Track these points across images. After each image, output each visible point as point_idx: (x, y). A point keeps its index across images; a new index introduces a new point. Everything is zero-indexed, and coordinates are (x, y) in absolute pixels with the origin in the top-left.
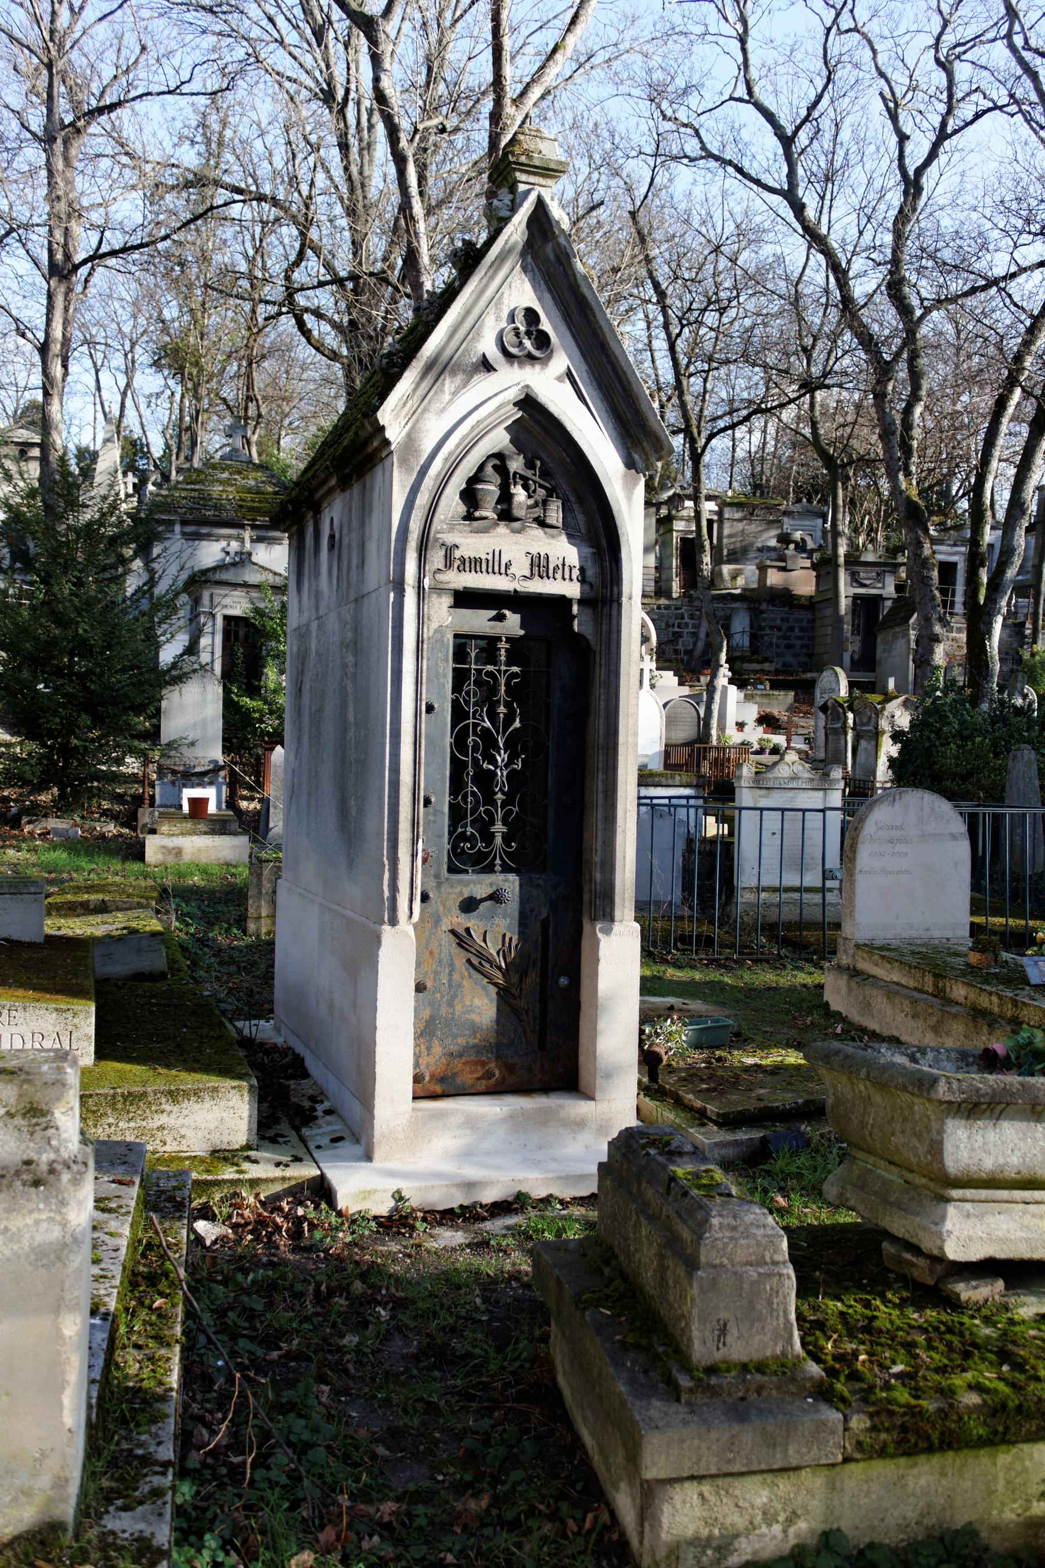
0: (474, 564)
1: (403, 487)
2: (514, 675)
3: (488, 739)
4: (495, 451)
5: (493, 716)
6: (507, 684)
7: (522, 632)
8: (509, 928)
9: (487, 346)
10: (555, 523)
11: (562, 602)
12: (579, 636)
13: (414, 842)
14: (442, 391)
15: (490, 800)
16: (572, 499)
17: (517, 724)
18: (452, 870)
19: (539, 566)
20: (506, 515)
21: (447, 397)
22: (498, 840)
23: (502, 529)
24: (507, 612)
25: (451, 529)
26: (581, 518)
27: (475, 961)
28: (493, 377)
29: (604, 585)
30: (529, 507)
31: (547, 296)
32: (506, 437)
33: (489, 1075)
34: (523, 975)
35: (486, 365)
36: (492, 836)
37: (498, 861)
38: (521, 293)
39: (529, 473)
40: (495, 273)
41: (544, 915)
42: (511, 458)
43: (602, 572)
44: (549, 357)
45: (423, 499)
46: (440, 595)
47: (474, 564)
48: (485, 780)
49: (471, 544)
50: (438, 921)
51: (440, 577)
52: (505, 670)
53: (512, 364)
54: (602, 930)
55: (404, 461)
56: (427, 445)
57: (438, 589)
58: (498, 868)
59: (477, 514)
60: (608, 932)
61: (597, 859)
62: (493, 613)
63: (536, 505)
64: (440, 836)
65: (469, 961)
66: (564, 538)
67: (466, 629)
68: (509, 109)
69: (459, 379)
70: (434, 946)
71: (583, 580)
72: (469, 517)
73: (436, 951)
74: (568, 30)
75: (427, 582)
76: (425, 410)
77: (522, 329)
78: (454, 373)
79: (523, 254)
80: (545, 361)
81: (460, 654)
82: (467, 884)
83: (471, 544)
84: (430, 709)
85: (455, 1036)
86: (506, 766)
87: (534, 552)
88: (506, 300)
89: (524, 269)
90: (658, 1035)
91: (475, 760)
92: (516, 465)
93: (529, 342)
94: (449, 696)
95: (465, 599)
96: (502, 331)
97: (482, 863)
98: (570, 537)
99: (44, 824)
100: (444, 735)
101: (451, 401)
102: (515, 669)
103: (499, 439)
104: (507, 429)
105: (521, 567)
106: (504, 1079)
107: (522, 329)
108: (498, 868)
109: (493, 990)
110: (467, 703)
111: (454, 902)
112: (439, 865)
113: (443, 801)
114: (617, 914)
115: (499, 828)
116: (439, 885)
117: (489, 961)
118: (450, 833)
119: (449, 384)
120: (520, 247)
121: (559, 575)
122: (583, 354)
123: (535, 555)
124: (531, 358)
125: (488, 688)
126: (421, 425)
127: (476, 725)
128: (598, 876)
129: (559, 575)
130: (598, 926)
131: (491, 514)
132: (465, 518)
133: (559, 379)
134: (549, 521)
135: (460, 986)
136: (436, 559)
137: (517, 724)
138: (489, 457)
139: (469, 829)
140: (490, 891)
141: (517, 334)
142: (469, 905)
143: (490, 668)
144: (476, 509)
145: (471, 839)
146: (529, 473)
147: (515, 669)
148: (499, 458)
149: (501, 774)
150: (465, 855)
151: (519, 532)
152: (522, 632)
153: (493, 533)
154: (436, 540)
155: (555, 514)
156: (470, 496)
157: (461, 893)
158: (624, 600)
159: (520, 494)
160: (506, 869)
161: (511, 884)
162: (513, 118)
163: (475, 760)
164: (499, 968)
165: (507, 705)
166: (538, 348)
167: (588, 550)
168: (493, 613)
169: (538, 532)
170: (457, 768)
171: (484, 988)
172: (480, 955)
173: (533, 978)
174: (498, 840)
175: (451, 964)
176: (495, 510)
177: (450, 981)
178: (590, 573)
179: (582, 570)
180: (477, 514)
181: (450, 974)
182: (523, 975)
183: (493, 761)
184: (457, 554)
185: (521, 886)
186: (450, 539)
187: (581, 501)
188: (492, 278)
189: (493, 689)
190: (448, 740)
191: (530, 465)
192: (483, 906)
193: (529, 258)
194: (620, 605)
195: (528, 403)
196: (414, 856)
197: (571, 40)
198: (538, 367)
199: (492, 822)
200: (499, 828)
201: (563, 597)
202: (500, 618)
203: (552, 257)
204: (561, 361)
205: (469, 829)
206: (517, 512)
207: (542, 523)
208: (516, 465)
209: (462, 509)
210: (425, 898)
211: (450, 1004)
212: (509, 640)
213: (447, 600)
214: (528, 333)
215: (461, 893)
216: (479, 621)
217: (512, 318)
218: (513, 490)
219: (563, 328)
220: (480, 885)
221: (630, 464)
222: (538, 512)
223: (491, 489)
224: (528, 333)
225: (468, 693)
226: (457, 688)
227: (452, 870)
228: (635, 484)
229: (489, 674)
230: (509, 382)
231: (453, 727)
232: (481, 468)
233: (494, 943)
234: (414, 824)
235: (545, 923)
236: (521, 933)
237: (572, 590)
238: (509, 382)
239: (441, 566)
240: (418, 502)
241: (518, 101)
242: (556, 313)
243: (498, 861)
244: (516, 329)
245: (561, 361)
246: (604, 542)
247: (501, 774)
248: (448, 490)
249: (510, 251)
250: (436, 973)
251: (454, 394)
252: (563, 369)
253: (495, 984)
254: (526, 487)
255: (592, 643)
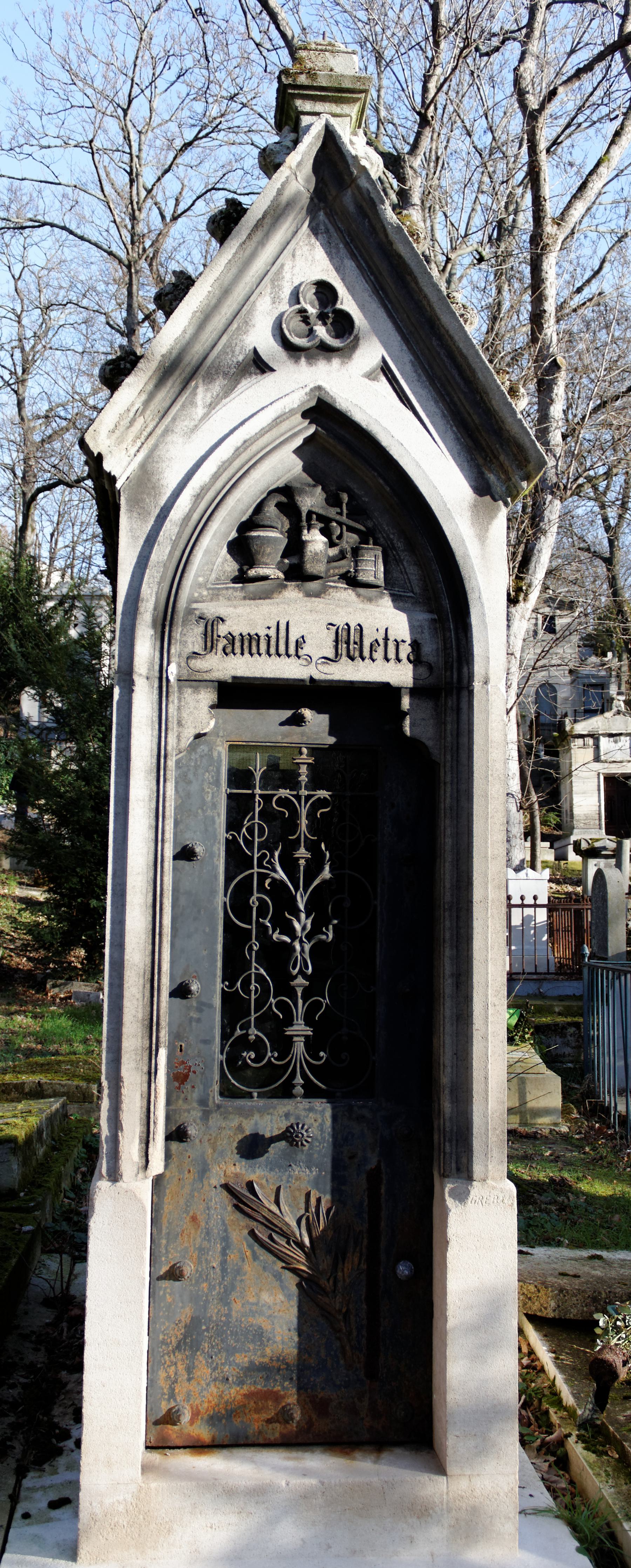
0: (249, 643)
1: (135, 538)
2: (322, 803)
3: (282, 899)
4: (280, 483)
5: (290, 865)
6: (311, 815)
7: (332, 740)
8: (316, 1183)
9: (260, 337)
10: (371, 579)
11: (386, 693)
12: (413, 741)
13: (152, 1053)
14: (193, 403)
15: (284, 987)
16: (399, 545)
17: (326, 873)
18: (228, 1092)
19: (348, 642)
20: (296, 572)
21: (200, 411)
22: (299, 1047)
23: (292, 593)
24: (307, 713)
25: (215, 595)
26: (413, 572)
27: (263, 1235)
28: (268, 379)
29: (448, 666)
30: (331, 560)
31: (350, 264)
32: (296, 466)
33: (284, 1416)
34: (339, 1256)
35: (259, 365)
36: (289, 1042)
37: (299, 1080)
38: (310, 262)
39: (332, 512)
40: (267, 236)
41: (373, 1163)
42: (301, 492)
43: (446, 648)
44: (353, 347)
45: (161, 553)
46: (196, 690)
47: (249, 643)
48: (277, 958)
49: (243, 615)
50: (204, 1171)
51: (197, 664)
52: (307, 798)
53: (297, 360)
54: (452, 1194)
55: (136, 503)
56: (170, 480)
57: (192, 681)
58: (299, 1090)
59: (252, 573)
60: (462, 1197)
61: (445, 1079)
62: (287, 714)
63: (342, 556)
64: (207, 1042)
65: (252, 1233)
66: (387, 602)
67: (245, 737)
68: (549, 229)
69: (217, 386)
70: (198, 1208)
71: (416, 659)
72: (241, 578)
73: (201, 1218)
74: (613, 142)
75: (173, 671)
76: (166, 431)
77: (312, 311)
78: (209, 378)
79: (312, 210)
80: (346, 353)
81: (239, 777)
82: (247, 1114)
83: (243, 615)
84: (185, 854)
85: (231, 1351)
86: (309, 937)
87: (340, 622)
88: (287, 274)
89: (315, 230)
90: (618, 1330)
91: (262, 928)
92: (311, 500)
93: (324, 328)
94: (222, 833)
95: (234, 694)
96: (281, 315)
97: (275, 1084)
98: (398, 600)
99: (69, 988)
100: (213, 892)
101: (206, 416)
102: (323, 794)
103: (284, 465)
104: (298, 451)
105: (320, 644)
106: (310, 1423)
107: (312, 311)
108: (299, 1090)
109: (291, 1281)
110: (249, 844)
111: (230, 1142)
112: (207, 1085)
113: (211, 988)
114: (477, 1169)
115: (299, 1029)
116: (206, 1115)
117: (283, 1234)
118: (225, 1037)
119: (202, 394)
120: (305, 200)
121: (379, 654)
122: (406, 340)
123: (344, 627)
124: (325, 350)
125: (281, 825)
126: (161, 451)
127: (262, 877)
128: (447, 1106)
129: (379, 654)
130: (448, 1187)
131: (272, 571)
132: (235, 580)
133: (370, 376)
134: (362, 577)
135: (238, 1271)
136: (190, 638)
137: (326, 873)
138: (270, 493)
139: (253, 1033)
140: (283, 1125)
141: (306, 319)
142: (252, 1147)
143: (284, 793)
144: (252, 564)
145: (258, 1046)
146: (332, 512)
147: (323, 794)
148: (285, 496)
149: (302, 949)
150: (251, 1071)
151: (317, 595)
152: (332, 740)
153: (278, 598)
154: (190, 611)
155: (372, 568)
156: (242, 548)
157: (240, 1128)
158: (477, 685)
159: (315, 541)
160: (311, 1092)
161: (316, 1118)
162: (555, 237)
163: (262, 928)
164: (300, 1245)
165: (312, 847)
166: (337, 336)
167: (423, 617)
168: (287, 714)
169: (347, 595)
170: (235, 939)
171: (278, 1277)
172: (269, 1225)
173: (353, 1264)
174: (299, 1047)
175: (226, 1239)
176: (279, 566)
177: (223, 1263)
178: (428, 649)
179: (415, 645)
180: (252, 573)
181: (224, 1253)
182: (339, 1256)
183: (290, 931)
184: (223, 630)
185: (334, 1118)
186: (211, 609)
187: (411, 547)
188: (262, 243)
189: (292, 824)
190: (220, 899)
191: (333, 500)
192: (276, 1149)
193: (322, 216)
194: (471, 693)
195: (323, 412)
196: (151, 1074)
197: (616, 152)
198: (336, 362)
199: (289, 1021)
200: (299, 1029)
201: (387, 685)
202: (297, 720)
203: (352, 208)
204: (371, 352)
205: (253, 1033)
206: (311, 567)
207: (352, 581)
208: (311, 500)
209: (231, 567)
210: (177, 1135)
211: (224, 1299)
212: (314, 751)
213: (208, 697)
214: (322, 317)
215: (240, 1128)
216: (265, 725)
217: (295, 297)
218: (306, 536)
219: (374, 305)
220: (270, 1118)
221: (482, 488)
222: (346, 565)
223: (273, 537)
224: (322, 317)
225: (250, 830)
226: (233, 824)
227: (228, 1092)
228: (491, 515)
229: (282, 802)
230: (291, 385)
231: (228, 880)
232: (259, 508)
233: (293, 1206)
234: (151, 1025)
235: (374, 1178)
236: (336, 1192)
237: (401, 674)
238: (291, 385)
239: (198, 648)
240: (153, 557)
241: (559, 221)
242: (362, 285)
243: (299, 1080)
244: (302, 311)
245: (371, 352)
246: (446, 603)
247: (302, 949)
248: (206, 541)
249: (290, 205)
250: (201, 1250)
251: (212, 406)
252: (376, 361)
253: (295, 1271)
254: (326, 532)
255: (435, 752)
